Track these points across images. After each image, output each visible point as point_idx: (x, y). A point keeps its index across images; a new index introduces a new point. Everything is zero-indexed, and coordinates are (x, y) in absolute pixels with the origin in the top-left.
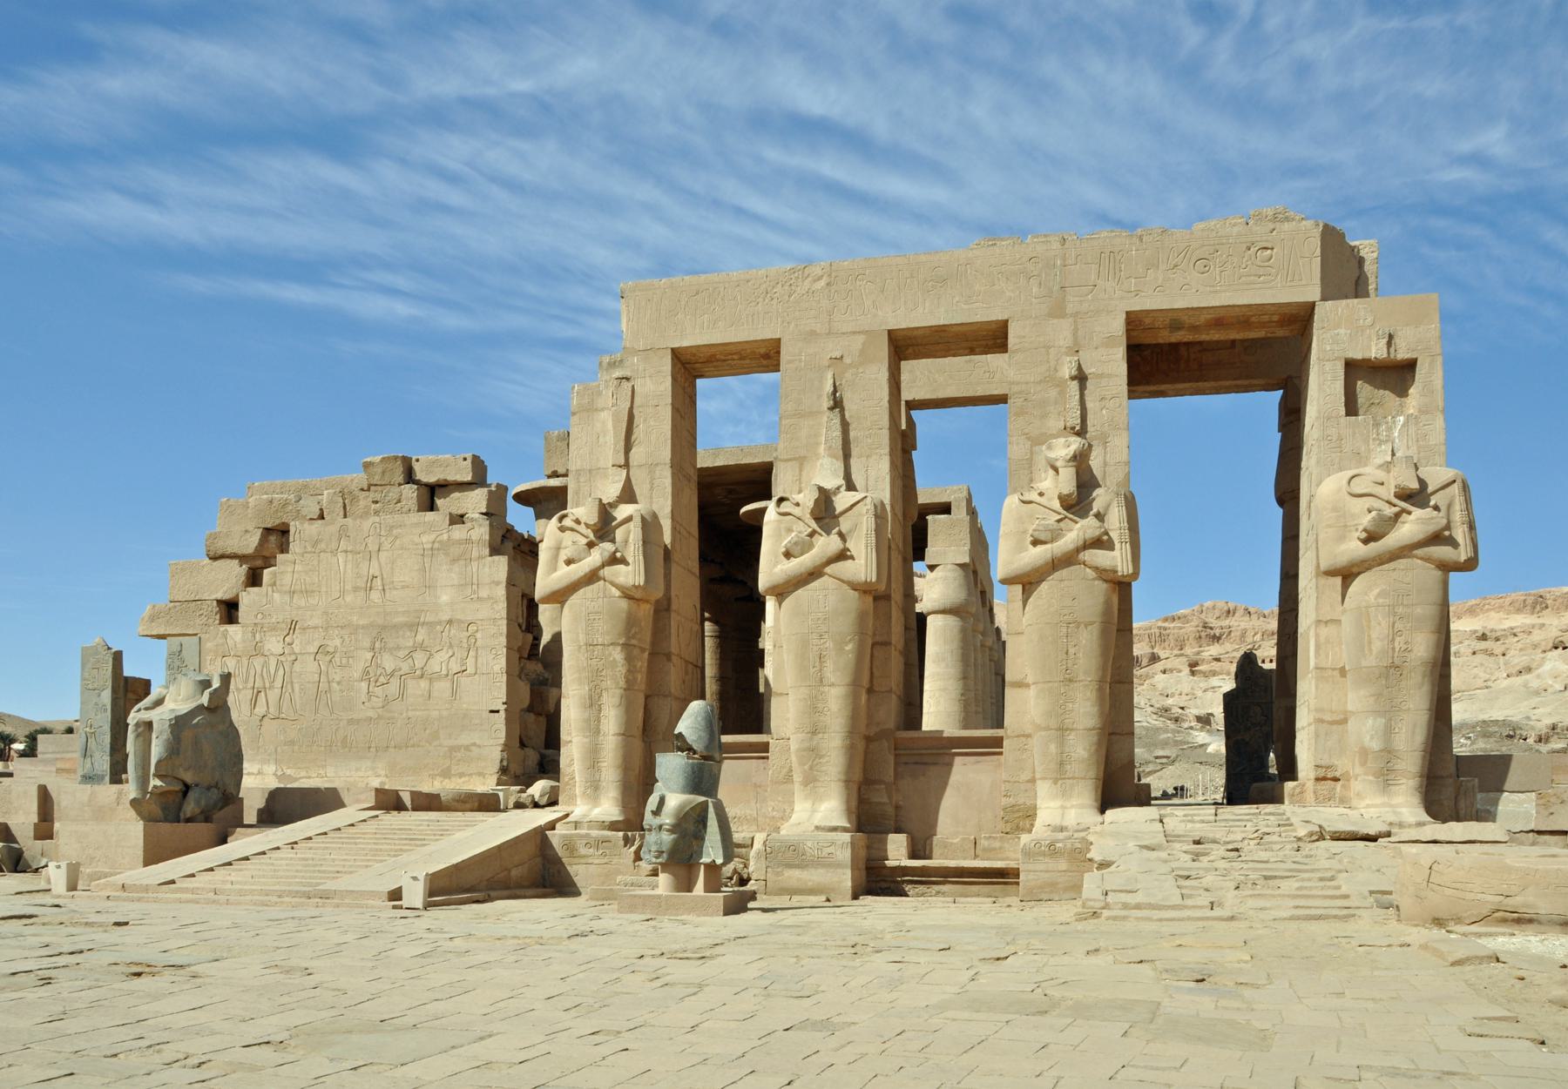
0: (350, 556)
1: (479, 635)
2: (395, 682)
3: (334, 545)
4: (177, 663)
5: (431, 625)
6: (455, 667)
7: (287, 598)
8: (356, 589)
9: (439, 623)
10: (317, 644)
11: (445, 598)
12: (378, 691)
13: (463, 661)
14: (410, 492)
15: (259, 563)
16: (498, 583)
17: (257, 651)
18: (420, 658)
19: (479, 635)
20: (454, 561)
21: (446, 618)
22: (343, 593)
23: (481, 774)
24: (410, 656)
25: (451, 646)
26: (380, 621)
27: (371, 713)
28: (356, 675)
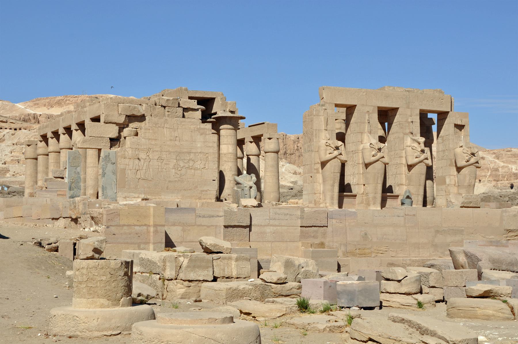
2: (184, 170)
5: (195, 153)
7: (147, 141)
8: (171, 140)
10: (158, 156)
12: (178, 172)
14: (180, 110)
15: (122, 126)
16: (215, 142)
18: (191, 164)
20: (201, 134)
23: (211, 199)
24: (188, 162)
25: (201, 160)
27: (176, 179)
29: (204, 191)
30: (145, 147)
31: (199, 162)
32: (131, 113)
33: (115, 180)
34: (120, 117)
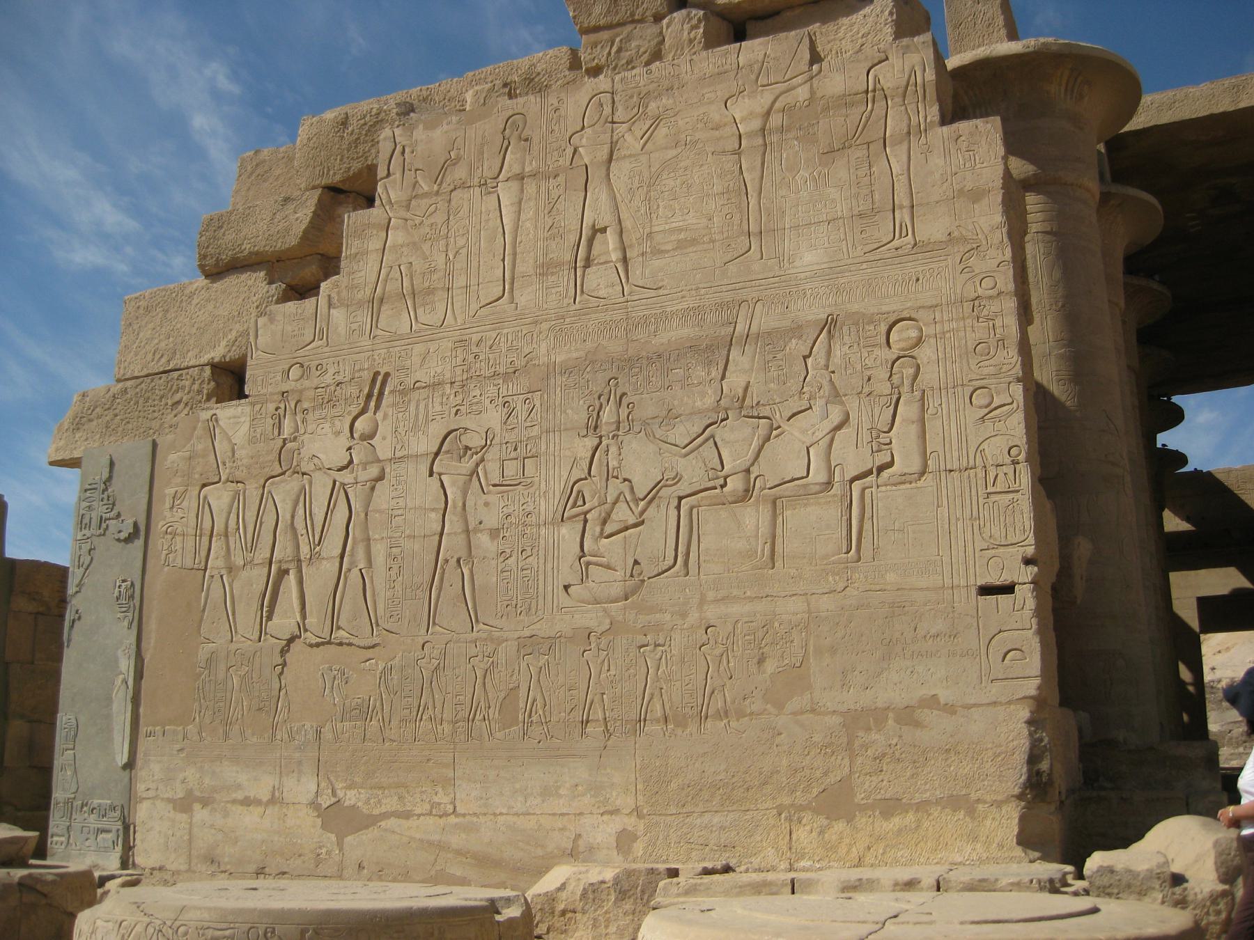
2: (661, 519)
4: (100, 509)
6: (852, 456)
7: (364, 317)
8: (546, 269)
9: (796, 330)
11: (809, 257)
13: (880, 439)
15: (310, 271)
16: (976, 196)
17: (286, 461)
18: (736, 442)
19: (925, 354)
20: (830, 153)
21: (816, 312)
22: (509, 284)
24: (706, 435)
25: (836, 396)
26: (614, 347)
27: (591, 618)
28: (547, 506)
29: (875, 716)
31: (816, 424)
33: (126, 665)
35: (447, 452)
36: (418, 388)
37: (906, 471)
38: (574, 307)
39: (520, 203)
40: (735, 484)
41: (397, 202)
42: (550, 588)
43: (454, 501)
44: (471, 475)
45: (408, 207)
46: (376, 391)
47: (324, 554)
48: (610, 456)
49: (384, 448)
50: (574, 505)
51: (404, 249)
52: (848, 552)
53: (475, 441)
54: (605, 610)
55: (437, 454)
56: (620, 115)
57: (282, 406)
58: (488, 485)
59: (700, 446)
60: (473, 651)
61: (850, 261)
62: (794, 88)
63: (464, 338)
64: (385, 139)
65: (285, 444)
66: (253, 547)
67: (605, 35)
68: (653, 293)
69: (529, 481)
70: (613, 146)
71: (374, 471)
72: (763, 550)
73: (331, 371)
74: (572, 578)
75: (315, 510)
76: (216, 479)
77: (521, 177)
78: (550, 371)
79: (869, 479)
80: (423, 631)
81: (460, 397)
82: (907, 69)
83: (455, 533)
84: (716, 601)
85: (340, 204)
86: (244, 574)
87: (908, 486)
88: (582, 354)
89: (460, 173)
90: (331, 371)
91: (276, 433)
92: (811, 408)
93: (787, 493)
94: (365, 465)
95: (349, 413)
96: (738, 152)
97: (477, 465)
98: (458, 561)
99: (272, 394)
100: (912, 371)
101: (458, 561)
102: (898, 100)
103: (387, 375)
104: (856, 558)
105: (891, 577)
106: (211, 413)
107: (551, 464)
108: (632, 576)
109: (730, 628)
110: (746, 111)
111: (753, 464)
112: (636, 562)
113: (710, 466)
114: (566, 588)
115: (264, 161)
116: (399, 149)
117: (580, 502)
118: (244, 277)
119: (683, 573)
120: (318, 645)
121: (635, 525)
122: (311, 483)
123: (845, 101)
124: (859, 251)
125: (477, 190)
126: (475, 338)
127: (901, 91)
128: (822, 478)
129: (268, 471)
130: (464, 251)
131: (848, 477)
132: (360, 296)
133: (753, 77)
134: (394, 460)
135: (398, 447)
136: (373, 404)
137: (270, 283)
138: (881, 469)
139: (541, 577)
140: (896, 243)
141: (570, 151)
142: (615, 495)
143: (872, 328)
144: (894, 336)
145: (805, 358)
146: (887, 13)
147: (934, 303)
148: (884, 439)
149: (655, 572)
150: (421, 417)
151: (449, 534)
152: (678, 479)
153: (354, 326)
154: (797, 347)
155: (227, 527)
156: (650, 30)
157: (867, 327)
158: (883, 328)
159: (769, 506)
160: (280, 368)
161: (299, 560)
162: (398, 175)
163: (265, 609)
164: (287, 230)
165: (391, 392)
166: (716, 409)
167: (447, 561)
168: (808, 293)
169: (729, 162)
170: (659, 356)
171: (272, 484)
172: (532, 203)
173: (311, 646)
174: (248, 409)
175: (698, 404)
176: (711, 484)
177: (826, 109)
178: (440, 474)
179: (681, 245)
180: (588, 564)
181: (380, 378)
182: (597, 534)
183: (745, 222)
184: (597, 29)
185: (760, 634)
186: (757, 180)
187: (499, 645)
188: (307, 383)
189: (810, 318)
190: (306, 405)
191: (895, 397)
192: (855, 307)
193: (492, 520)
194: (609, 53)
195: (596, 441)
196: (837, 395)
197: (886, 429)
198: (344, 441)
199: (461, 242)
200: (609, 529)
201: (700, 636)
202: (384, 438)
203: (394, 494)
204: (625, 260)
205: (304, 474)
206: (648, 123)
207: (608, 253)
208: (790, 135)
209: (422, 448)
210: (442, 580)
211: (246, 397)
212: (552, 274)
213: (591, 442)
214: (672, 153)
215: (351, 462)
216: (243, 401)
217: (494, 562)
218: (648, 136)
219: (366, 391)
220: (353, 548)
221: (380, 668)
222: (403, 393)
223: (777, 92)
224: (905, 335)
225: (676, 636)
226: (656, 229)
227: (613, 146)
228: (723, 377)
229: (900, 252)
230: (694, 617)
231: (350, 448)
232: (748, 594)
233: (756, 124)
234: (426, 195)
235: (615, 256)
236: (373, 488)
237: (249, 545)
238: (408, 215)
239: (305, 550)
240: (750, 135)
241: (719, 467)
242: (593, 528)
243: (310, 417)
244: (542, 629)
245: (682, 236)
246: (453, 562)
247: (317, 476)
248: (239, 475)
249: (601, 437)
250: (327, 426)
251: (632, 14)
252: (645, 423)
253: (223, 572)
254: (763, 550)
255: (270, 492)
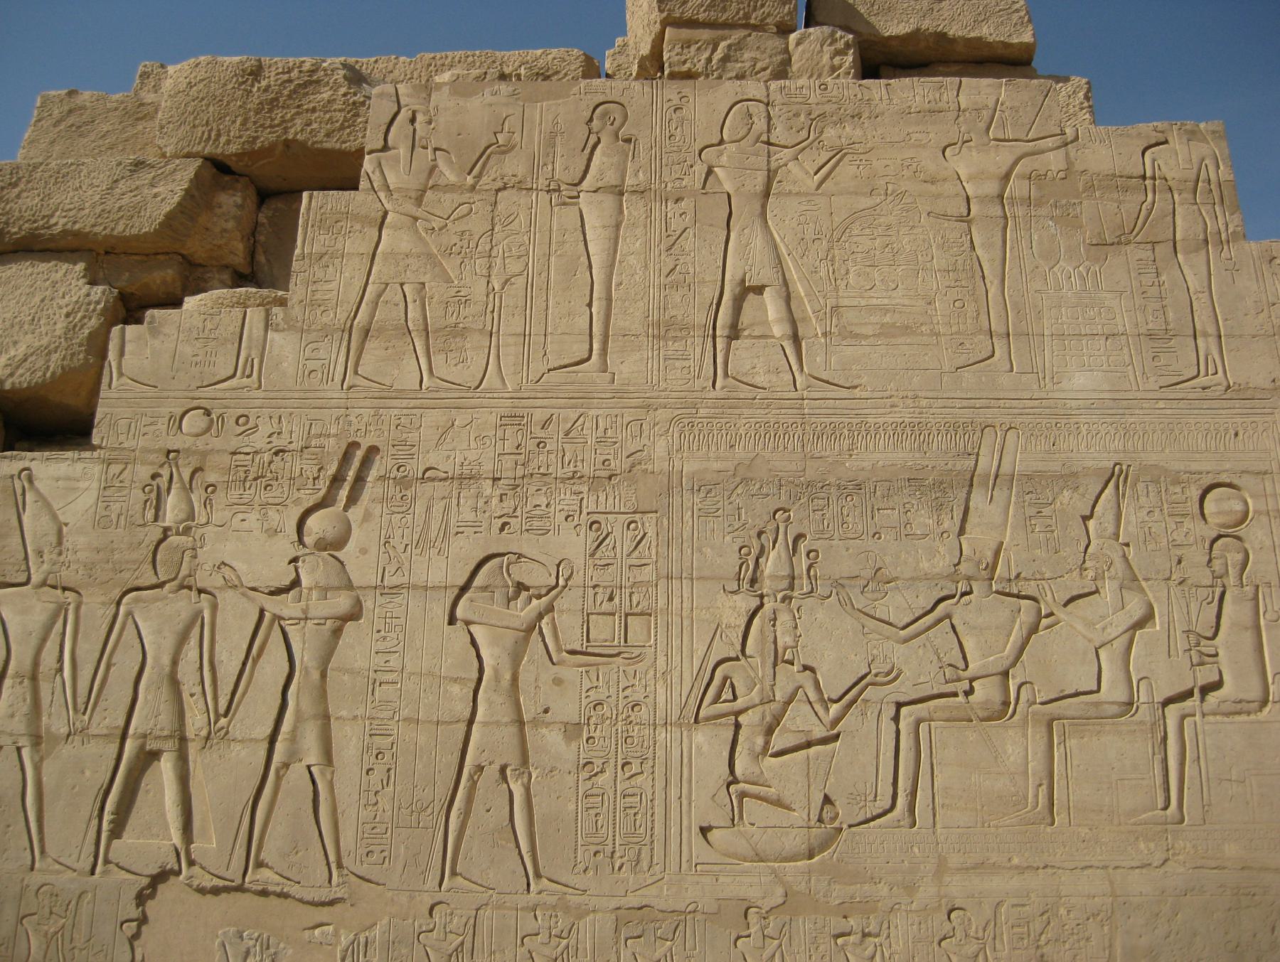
0: (633, 209)
1: (1255, 534)
2: (868, 736)
3: (564, 166)
5: (1033, 484)
7: (334, 354)
8: (664, 330)
9: (1069, 479)
10: (467, 549)
12: (784, 775)
13: (1202, 644)
17: (164, 564)
18: (985, 629)
22: (601, 342)
27: (752, 884)
28: (669, 695)
30: (294, 434)
31: (1110, 611)
32: (266, 138)
34: (146, 176)
35: (484, 588)
36: (433, 480)
37: (1241, 696)
38: (713, 394)
39: (618, 226)
40: (985, 692)
41: (399, 190)
42: (674, 830)
43: (496, 671)
44: (530, 630)
45: (419, 201)
46: (351, 474)
47: (237, 731)
48: (778, 628)
49: (360, 560)
50: (716, 700)
51: (410, 261)
52: (1166, 808)
53: (538, 577)
54: (774, 871)
55: (464, 589)
56: (779, 135)
57: (165, 472)
58: (559, 650)
59: (929, 628)
60: (531, 926)
61: (1139, 395)
62: (1043, 152)
63: (519, 412)
64: (381, 95)
65: (165, 537)
66: (89, 702)
67: (705, 34)
68: (844, 393)
69: (636, 652)
70: (770, 176)
71: (342, 602)
72: (1036, 796)
73: (264, 429)
74: (717, 817)
75: (222, 655)
76: (23, 578)
77: (619, 192)
78: (671, 484)
79: (1188, 703)
80: (432, 882)
81: (508, 504)
82: (1195, 160)
83: (498, 723)
84: (964, 870)
85: (224, 189)
86: (66, 750)
87: (1244, 718)
88: (730, 465)
89: (514, 166)
90: (264, 429)
91: (150, 515)
92: (1097, 591)
93: (1070, 713)
94: (325, 591)
95: (297, 502)
96: (966, 219)
97: (540, 616)
98: (503, 770)
99: (149, 451)
100: (1240, 557)
101: (503, 770)
102: (1189, 196)
103: (373, 450)
104: (1178, 817)
105: (1231, 850)
106: (21, 465)
107: (675, 630)
108: (820, 820)
109: (988, 913)
110: (973, 167)
111: (1014, 664)
112: (827, 800)
113: (946, 660)
114: (704, 831)
115: (83, 108)
116: (404, 114)
117: (727, 694)
118: (43, 267)
119: (907, 821)
120: (216, 891)
121: (824, 741)
122: (214, 608)
123: (1117, 183)
124: (1152, 383)
125: (544, 197)
126: (539, 415)
127: (1190, 185)
128: (1123, 697)
129: (129, 578)
130: (520, 281)
131: (1159, 698)
132: (325, 319)
133: (982, 125)
134: (381, 589)
135: (391, 569)
136: (343, 494)
137: (93, 283)
138: (1206, 690)
139: (659, 811)
140: (1202, 380)
141: (700, 169)
142: (790, 689)
143: (1178, 489)
144: (1209, 506)
145: (1085, 519)
146: (1081, 95)
147: (1263, 468)
148: (1207, 647)
149: (861, 818)
150: (434, 526)
151: (485, 724)
152: (893, 675)
153: (311, 365)
154: (1071, 501)
155: (36, 664)
156: (775, 43)
157: (1171, 488)
158: (1195, 493)
159: (1044, 729)
160: (165, 411)
161: (183, 740)
162: (403, 151)
163: (107, 817)
164: (138, 209)
165: (382, 478)
166: (953, 577)
167: (480, 768)
168: (1084, 429)
169: (954, 231)
170: (859, 487)
171: (137, 600)
172: (639, 231)
173: (201, 891)
174: (97, 469)
175: (925, 565)
176: (950, 688)
177: (1090, 188)
178: (468, 623)
179: (886, 332)
180: (743, 795)
181: (359, 454)
182: (758, 749)
183: (984, 317)
184: (692, 24)
185: (1037, 926)
186: (998, 262)
187: (580, 917)
188: (216, 443)
189: (1090, 464)
190: (212, 477)
191: (1218, 591)
192: (1152, 458)
193: (567, 708)
194: (709, 60)
195: (755, 602)
196: (1135, 579)
197: (1209, 634)
198: (285, 546)
199: (514, 267)
200: (778, 742)
201: (938, 923)
202: (364, 551)
203: (381, 646)
204: (796, 339)
205: (200, 591)
206: (825, 156)
207: (765, 323)
208: (1043, 211)
209: (436, 577)
210: (469, 800)
211: (94, 448)
212: (675, 339)
213: (745, 602)
214: (866, 202)
215: (296, 583)
216: (87, 454)
217: (571, 780)
218: (826, 172)
219: (332, 469)
220: (294, 730)
221: (344, 940)
222: (404, 483)
223: (1019, 152)
224: (1225, 506)
225: (898, 919)
226: (846, 302)
227: (770, 176)
228: (962, 531)
229: (1208, 393)
230: (926, 892)
231: (295, 560)
232: (1016, 861)
233: (991, 188)
234: (450, 188)
235: (779, 330)
236: (337, 632)
237: (81, 700)
238: (419, 212)
239: (196, 722)
240: (983, 199)
241: (961, 664)
242: (750, 739)
243: (219, 498)
244: (662, 897)
245: (887, 319)
246: (492, 771)
247: (227, 599)
248: (67, 576)
249: (762, 597)
250: (253, 517)
251: (747, 16)
252: (838, 584)
253: (23, 742)
254: (1036, 796)
255: (129, 614)
